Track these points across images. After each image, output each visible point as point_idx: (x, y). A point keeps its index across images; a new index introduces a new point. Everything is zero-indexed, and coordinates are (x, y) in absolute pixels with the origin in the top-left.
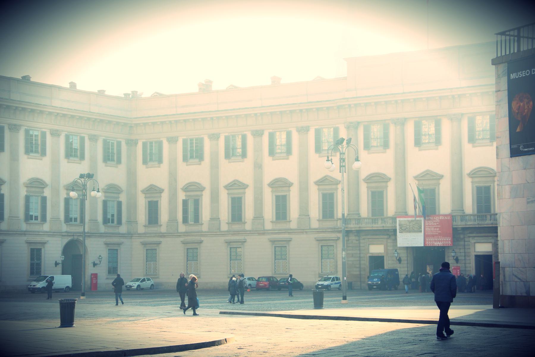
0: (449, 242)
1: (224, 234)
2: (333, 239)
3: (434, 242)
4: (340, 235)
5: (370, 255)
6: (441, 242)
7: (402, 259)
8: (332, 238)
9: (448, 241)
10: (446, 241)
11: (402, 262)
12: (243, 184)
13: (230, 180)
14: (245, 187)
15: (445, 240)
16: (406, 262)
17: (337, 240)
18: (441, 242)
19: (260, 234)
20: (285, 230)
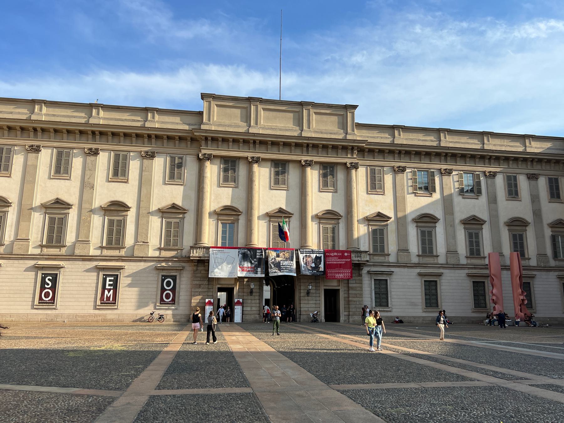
0: (350, 274)
1: (33, 257)
2: (178, 268)
3: (335, 274)
4: (183, 264)
5: (219, 286)
6: (341, 274)
7: (254, 291)
8: (176, 267)
9: (348, 273)
10: (346, 273)
11: (254, 294)
12: (69, 205)
13: (50, 197)
14: (68, 206)
15: (331, 272)
16: (258, 294)
17: (181, 270)
18: (341, 274)
19: (84, 260)
20: (119, 257)
